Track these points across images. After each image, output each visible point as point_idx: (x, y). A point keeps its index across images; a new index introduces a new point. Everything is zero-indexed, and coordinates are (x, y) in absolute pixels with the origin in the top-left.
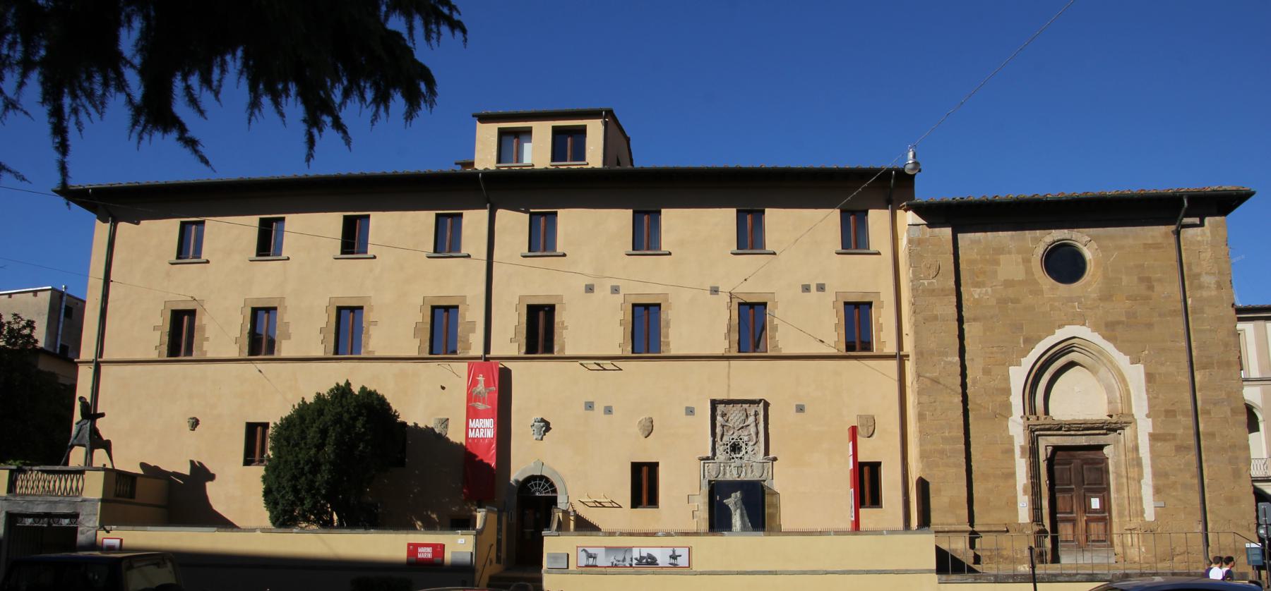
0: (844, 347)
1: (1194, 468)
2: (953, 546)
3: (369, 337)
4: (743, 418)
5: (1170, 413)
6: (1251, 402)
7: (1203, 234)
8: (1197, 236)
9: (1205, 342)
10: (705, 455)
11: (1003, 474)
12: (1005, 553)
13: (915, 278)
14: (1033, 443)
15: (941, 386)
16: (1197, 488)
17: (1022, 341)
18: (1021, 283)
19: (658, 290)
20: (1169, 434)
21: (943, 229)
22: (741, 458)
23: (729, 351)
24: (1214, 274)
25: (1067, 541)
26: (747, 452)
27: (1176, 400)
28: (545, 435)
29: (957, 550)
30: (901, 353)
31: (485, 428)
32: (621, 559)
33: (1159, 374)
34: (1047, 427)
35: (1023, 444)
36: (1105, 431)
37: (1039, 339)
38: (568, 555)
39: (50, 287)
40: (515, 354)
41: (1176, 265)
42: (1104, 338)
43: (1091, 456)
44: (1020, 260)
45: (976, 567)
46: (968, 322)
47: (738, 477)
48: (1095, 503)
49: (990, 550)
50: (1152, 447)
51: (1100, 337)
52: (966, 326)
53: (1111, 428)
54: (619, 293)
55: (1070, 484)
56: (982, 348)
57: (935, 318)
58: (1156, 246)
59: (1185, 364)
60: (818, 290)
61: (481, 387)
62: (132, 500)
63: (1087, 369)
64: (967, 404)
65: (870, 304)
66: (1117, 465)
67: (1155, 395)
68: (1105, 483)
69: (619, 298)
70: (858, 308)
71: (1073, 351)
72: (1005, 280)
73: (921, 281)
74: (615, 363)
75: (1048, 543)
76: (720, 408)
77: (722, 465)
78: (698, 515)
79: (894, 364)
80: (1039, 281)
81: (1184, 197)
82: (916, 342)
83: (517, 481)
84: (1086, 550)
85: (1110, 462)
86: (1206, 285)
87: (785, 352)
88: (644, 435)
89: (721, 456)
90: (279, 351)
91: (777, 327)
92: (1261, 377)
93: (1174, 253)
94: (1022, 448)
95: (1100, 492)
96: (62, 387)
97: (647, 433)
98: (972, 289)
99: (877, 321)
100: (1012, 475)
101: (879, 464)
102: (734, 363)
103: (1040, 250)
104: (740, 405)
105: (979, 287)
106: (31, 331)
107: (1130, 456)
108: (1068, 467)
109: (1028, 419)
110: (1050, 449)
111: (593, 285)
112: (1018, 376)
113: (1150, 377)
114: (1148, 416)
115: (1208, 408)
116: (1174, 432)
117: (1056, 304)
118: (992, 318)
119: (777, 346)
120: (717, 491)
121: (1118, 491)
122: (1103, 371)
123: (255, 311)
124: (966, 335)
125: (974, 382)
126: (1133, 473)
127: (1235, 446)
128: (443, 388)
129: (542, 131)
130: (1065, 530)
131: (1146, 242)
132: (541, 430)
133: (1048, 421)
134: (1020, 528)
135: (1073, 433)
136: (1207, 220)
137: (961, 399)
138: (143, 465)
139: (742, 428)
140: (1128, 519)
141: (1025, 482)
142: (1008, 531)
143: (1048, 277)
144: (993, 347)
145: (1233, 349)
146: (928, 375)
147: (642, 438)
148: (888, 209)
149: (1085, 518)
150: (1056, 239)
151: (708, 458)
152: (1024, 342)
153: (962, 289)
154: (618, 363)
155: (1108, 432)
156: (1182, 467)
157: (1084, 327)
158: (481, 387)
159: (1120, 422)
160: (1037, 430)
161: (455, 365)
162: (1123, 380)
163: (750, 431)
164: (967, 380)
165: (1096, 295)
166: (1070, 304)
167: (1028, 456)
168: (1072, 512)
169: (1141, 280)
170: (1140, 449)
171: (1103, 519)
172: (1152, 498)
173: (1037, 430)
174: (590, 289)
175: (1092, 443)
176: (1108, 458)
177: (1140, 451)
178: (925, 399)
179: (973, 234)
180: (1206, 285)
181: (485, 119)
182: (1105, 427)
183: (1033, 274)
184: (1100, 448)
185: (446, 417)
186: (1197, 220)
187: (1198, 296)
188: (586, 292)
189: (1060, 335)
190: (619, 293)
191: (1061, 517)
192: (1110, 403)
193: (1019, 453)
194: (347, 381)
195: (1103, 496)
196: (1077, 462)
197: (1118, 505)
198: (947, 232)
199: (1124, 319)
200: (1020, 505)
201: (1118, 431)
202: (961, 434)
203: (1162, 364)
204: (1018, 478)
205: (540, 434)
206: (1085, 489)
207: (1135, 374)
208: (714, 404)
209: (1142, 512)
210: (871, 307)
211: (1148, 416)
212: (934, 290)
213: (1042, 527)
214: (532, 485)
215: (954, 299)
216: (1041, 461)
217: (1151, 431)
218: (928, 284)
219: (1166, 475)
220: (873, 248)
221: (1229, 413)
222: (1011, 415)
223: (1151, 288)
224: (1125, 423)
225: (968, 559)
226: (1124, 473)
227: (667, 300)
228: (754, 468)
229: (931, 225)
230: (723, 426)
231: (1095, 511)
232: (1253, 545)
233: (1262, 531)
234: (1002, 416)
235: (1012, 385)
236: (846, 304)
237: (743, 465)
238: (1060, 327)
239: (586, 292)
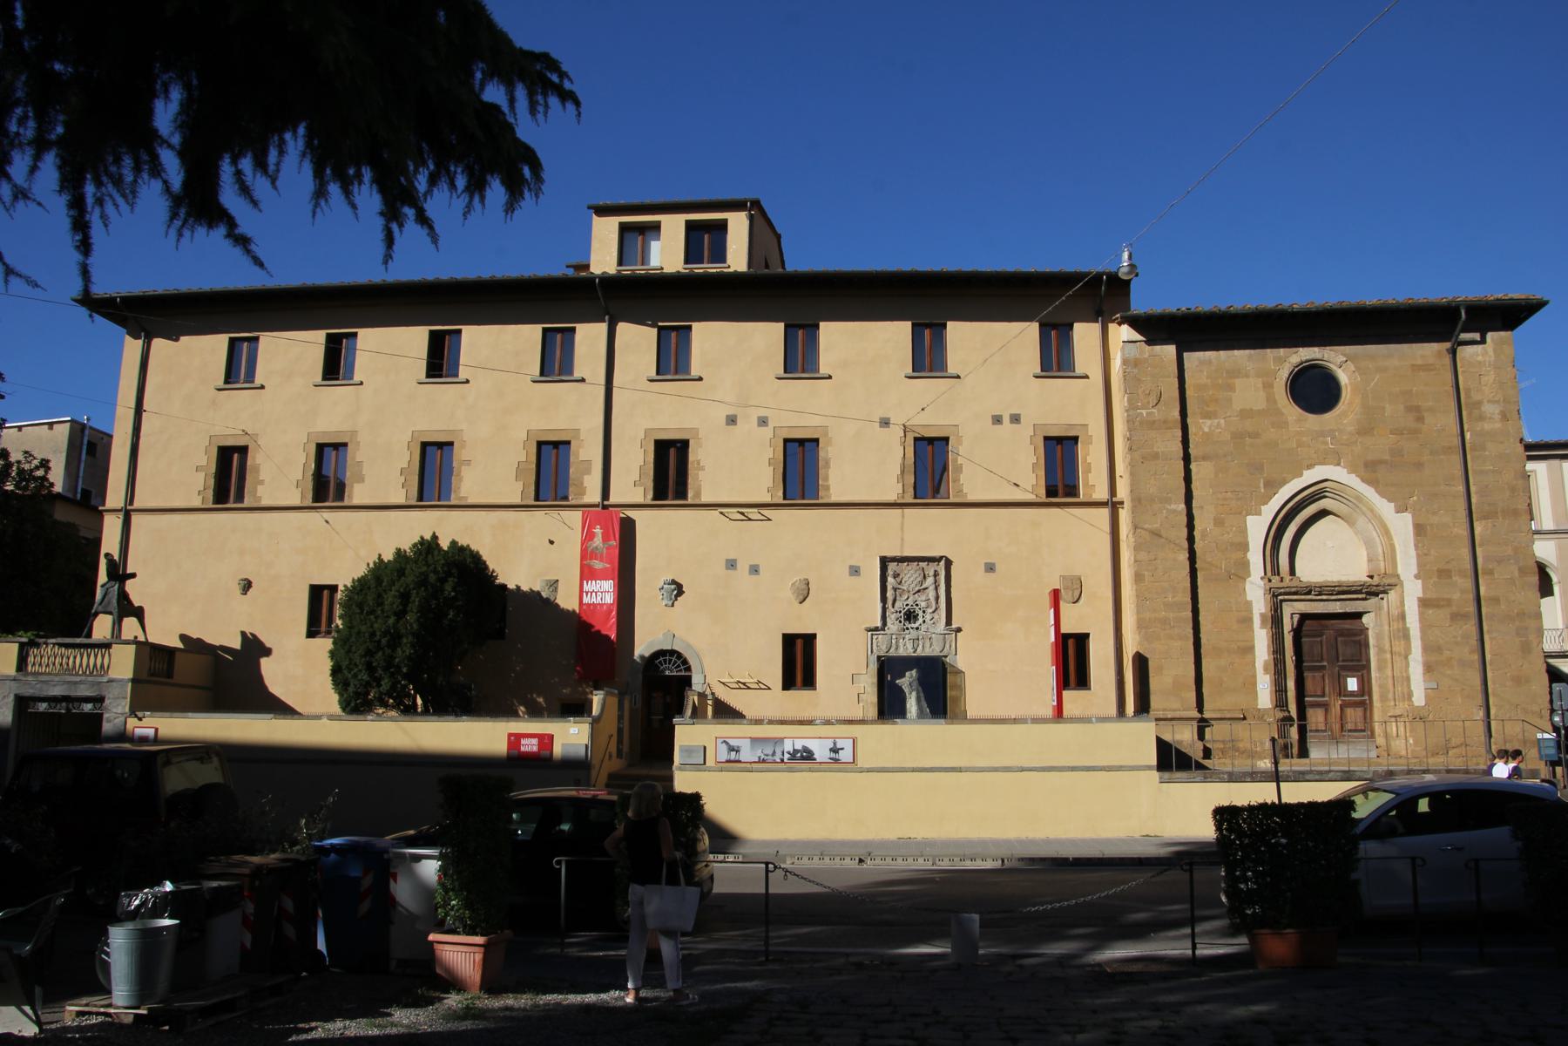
0: (1044, 492)
1: (1474, 642)
2: (1178, 737)
3: (461, 480)
4: (919, 579)
5: (1444, 574)
6: (1543, 559)
7: (1485, 353)
8: (1478, 355)
9: (1487, 486)
10: (873, 625)
11: (1239, 647)
12: (1241, 745)
13: (1131, 407)
14: (1276, 611)
15: (1163, 540)
16: (1477, 665)
17: (1262, 485)
18: (1260, 412)
19: (816, 421)
20: (1443, 599)
21: (1165, 347)
22: (917, 629)
23: (903, 497)
24: (1498, 402)
25: (1317, 731)
26: (924, 622)
27: (1452, 557)
28: (676, 600)
29: (1182, 741)
30: (1114, 499)
31: (603, 592)
32: (770, 752)
34: (1293, 590)
35: (1263, 611)
36: (1364, 596)
37: (1284, 482)
38: (705, 748)
39: (69, 419)
40: (640, 500)
41: (1452, 391)
43: (1347, 626)
44: (1260, 385)
45: (1206, 762)
46: (1196, 461)
47: (914, 652)
48: (1352, 684)
49: (1223, 742)
50: (1421, 614)
51: (1358, 480)
52: (1193, 466)
53: (1372, 591)
54: (767, 426)
55: (1322, 660)
56: (1213, 493)
57: (1156, 456)
58: (1426, 368)
59: (1463, 513)
60: (1012, 422)
61: (598, 541)
62: (168, 680)
63: (1343, 519)
64: (1196, 563)
65: (1075, 439)
66: (1379, 637)
67: (1426, 551)
68: (1364, 658)
69: (767, 432)
70: (1062, 444)
71: (1325, 497)
72: (1241, 411)
74: (762, 512)
75: (1294, 732)
76: (892, 567)
77: (894, 637)
78: (864, 698)
79: (1105, 513)
80: (1284, 410)
81: (1461, 307)
82: (1132, 485)
83: (642, 657)
84: (1342, 742)
85: (1371, 633)
86: (1489, 415)
87: (971, 498)
88: (798, 601)
89: (893, 626)
90: (350, 497)
92: (1555, 528)
93: (1449, 376)
94: (1262, 615)
95: (1358, 671)
96: (83, 541)
97: (801, 598)
98: (1201, 421)
99: (1085, 460)
100: (1250, 649)
101: (1087, 635)
102: (908, 511)
103: (1284, 373)
104: (916, 563)
105: (1210, 418)
106: (46, 472)
107: (1395, 625)
108: (1319, 639)
109: (1270, 581)
110: (1296, 618)
111: (736, 416)
112: (1257, 528)
113: (1419, 529)
114: (1417, 577)
115: (1491, 567)
116: (1448, 596)
117: (1304, 439)
119: (962, 491)
120: (888, 669)
121: (1380, 669)
122: (1361, 522)
123: (321, 448)
124: (1194, 477)
125: (1204, 536)
126: (1399, 646)
127: (1524, 614)
128: (552, 542)
129: (673, 227)
130: (1315, 717)
131: (1414, 363)
132: (672, 594)
133: (1295, 583)
134: (1260, 715)
135: (1324, 597)
136: (1489, 336)
137: (1188, 555)
138: (183, 638)
139: (919, 591)
140: (1392, 703)
141: (1266, 658)
142: (1244, 718)
143: (1296, 407)
145: (1521, 494)
146: (1146, 526)
147: (796, 603)
148: (1098, 322)
149: (1340, 702)
150: (1304, 359)
151: (876, 629)
152: (1264, 487)
153: (1189, 421)
154: (767, 512)
156: (1459, 639)
157: (1338, 468)
158: (598, 541)
159: (1382, 584)
160: (1280, 594)
161: (566, 514)
162: (1387, 533)
163: (928, 596)
164: (1195, 533)
165: (1353, 428)
166: (1321, 439)
167: (1270, 626)
168: (1323, 695)
169: (1409, 409)
170: (1407, 617)
171: (1362, 704)
173: (1280, 594)
174: (732, 420)
175: (1348, 610)
176: (1367, 629)
177: (1408, 620)
178: (1143, 556)
179: (1202, 353)
180: (1489, 415)
181: (603, 211)
182: (1364, 591)
183: (1275, 402)
184: (1358, 616)
185: (556, 578)
186: (1477, 336)
187: (1478, 429)
188: (728, 424)
190: (767, 426)
191: (1310, 702)
192: (1370, 560)
193: (1259, 622)
194: (434, 533)
195: (1362, 675)
196: (1329, 633)
197: (1380, 686)
198: (1171, 350)
199: (1387, 457)
200: (1260, 686)
201: (1381, 596)
202: (1188, 599)
203: (1434, 513)
204: (1257, 653)
205: (671, 599)
206: (1340, 666)
207: (1401, 526)
208: (884, 562)
209: (1410, 695)
210: (1077, 443)
211: (1417, 577)
212: (1154, 422)
213: (1286, 714)
214: (660, 662)
215: (1179, 433)
216: (1286, 632)
217: (1421, 595)
218: (1147, 414)
219: (1439, 649)
220: (1079, 371)
221: (1516, 574)
222: (1249, 576)
223: (1420, 419)
224: (1389, 585)
225: (1196, 753)
226: (1387, 647)
227: (826, 434)
228: (934, 641)
229: (1150, 342)
230: (895, 589)
231: (1352, 694)
232: (1546, 736)
233: (1557, 719)
234: (1237, 575)
235: (1250, 539)
236: (1046, 438)
237: (921, 637)
238: (1309, 467)
239: (728, 424)
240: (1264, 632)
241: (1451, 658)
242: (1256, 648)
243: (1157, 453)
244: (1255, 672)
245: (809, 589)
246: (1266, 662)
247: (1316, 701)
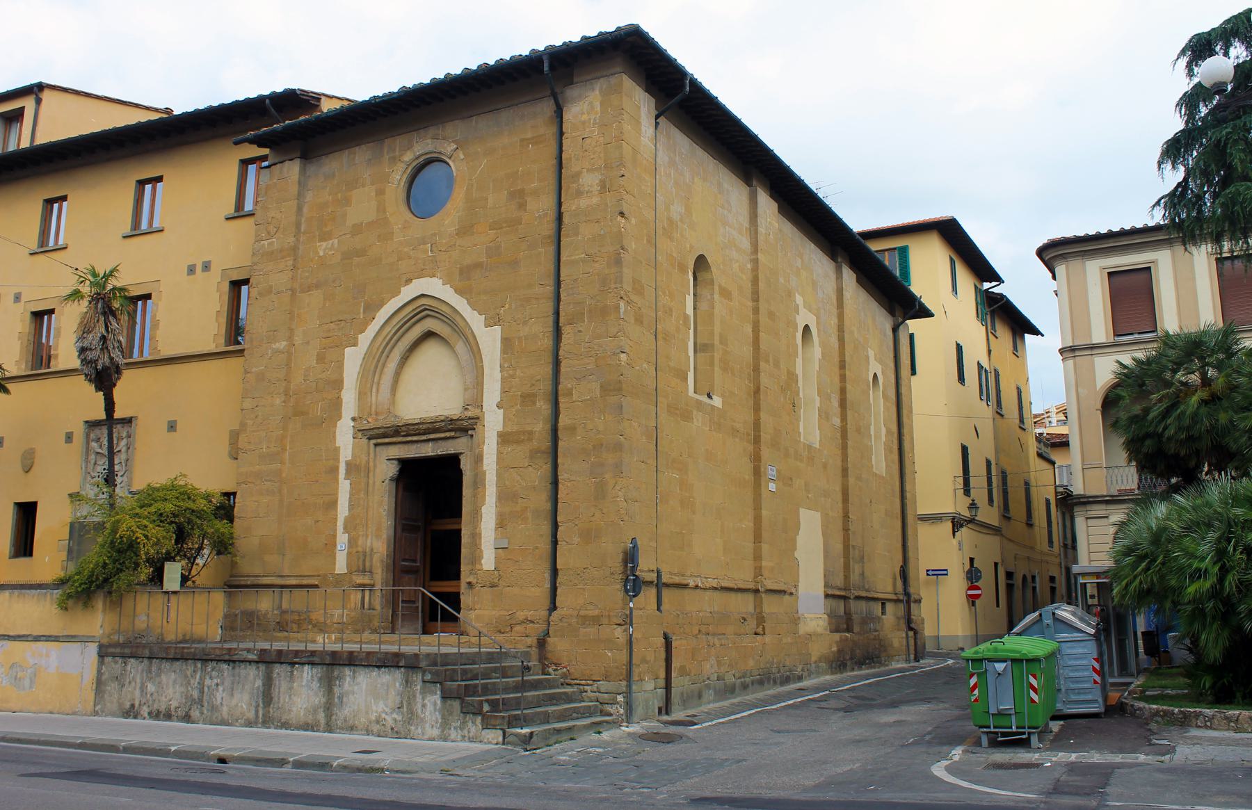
5: (528, 398)
8: (583, 113)
17: (362, 311)
20: (524, 432)
27: (538, 377)
33: (520, 338)
36: (453, 434)
42: (456, 292)
44: (373, 194)
50: (499, 453)
72: (354, 226)
73: (262, 242)
86: (586, 189)
91: (159, 323)
98: (318, 244)
100: (333, 504)
113: (507, 343)
114: (499, 406)
115: (569, 386)
117: (406, 249)
118: (334, 281)
135: (415, 438)
144: (331, 322)
152: (364, 312)
157: (435, 279)
169: (512, 195)
172: (493, 533)
177: (485, 461)
183: (384, 211)
189: (408, 293)
193: (344, 472)
201: (470, 432)
207: (489, 340)
212: (272, 252)
218: (269, 244)
222: (340, 417)
223: (522, 206)
235: (345, 375)
238: (409, 281)
240: (348, 482)
241: (527, 508)
242: (339, 502)
243: (271, 287)
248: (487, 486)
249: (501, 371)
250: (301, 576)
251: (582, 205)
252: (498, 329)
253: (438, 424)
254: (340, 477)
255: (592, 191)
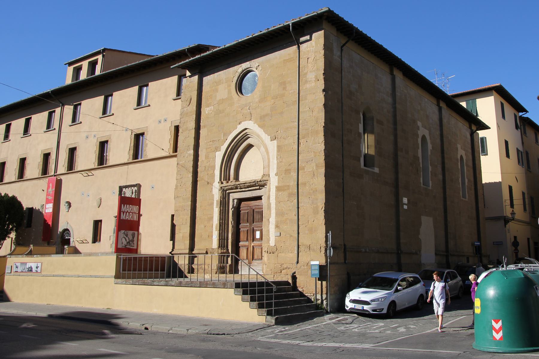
5: (287, 171)
27: (292, 162)
34: (230, 187)
35: (218, 199)
36: (258, 187)
53: (260, 185)
67: (281, 160)
86: (310, 80)
88: (97, 207)
94: (217, 201)
97: (98, 205)
100: (211, 218)
110: (236, 201)
113: (279, 148)
130: (243, 253)
135: (243, 190)
155: (261, 188)
159: (262, 180)
160: (226, 190)
173: (226, 190)
177: (271, 199)
184: (259, 198)
186: (308, 37)
193: (216, 205)
211: (276, 175)
231: (258, 240)
240: (217, 209)
244: (213, 230)
245: (101, 202)
246: (216, 224)
247: (244, 244)
248: (272, 210)
249: (277, 160)
250: (199, 249)
251: (308, 87)
252: (275, 141)
253: (252, 183)
254: (214, 207)
255: (312, 81)
